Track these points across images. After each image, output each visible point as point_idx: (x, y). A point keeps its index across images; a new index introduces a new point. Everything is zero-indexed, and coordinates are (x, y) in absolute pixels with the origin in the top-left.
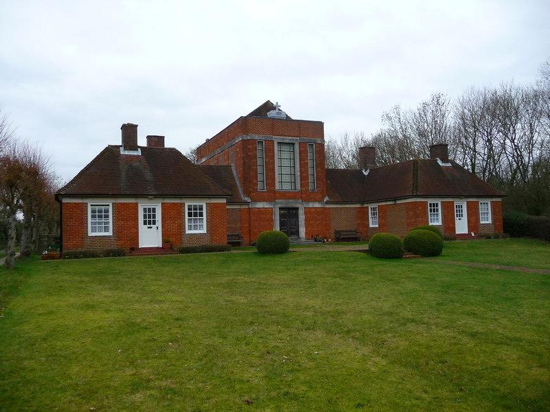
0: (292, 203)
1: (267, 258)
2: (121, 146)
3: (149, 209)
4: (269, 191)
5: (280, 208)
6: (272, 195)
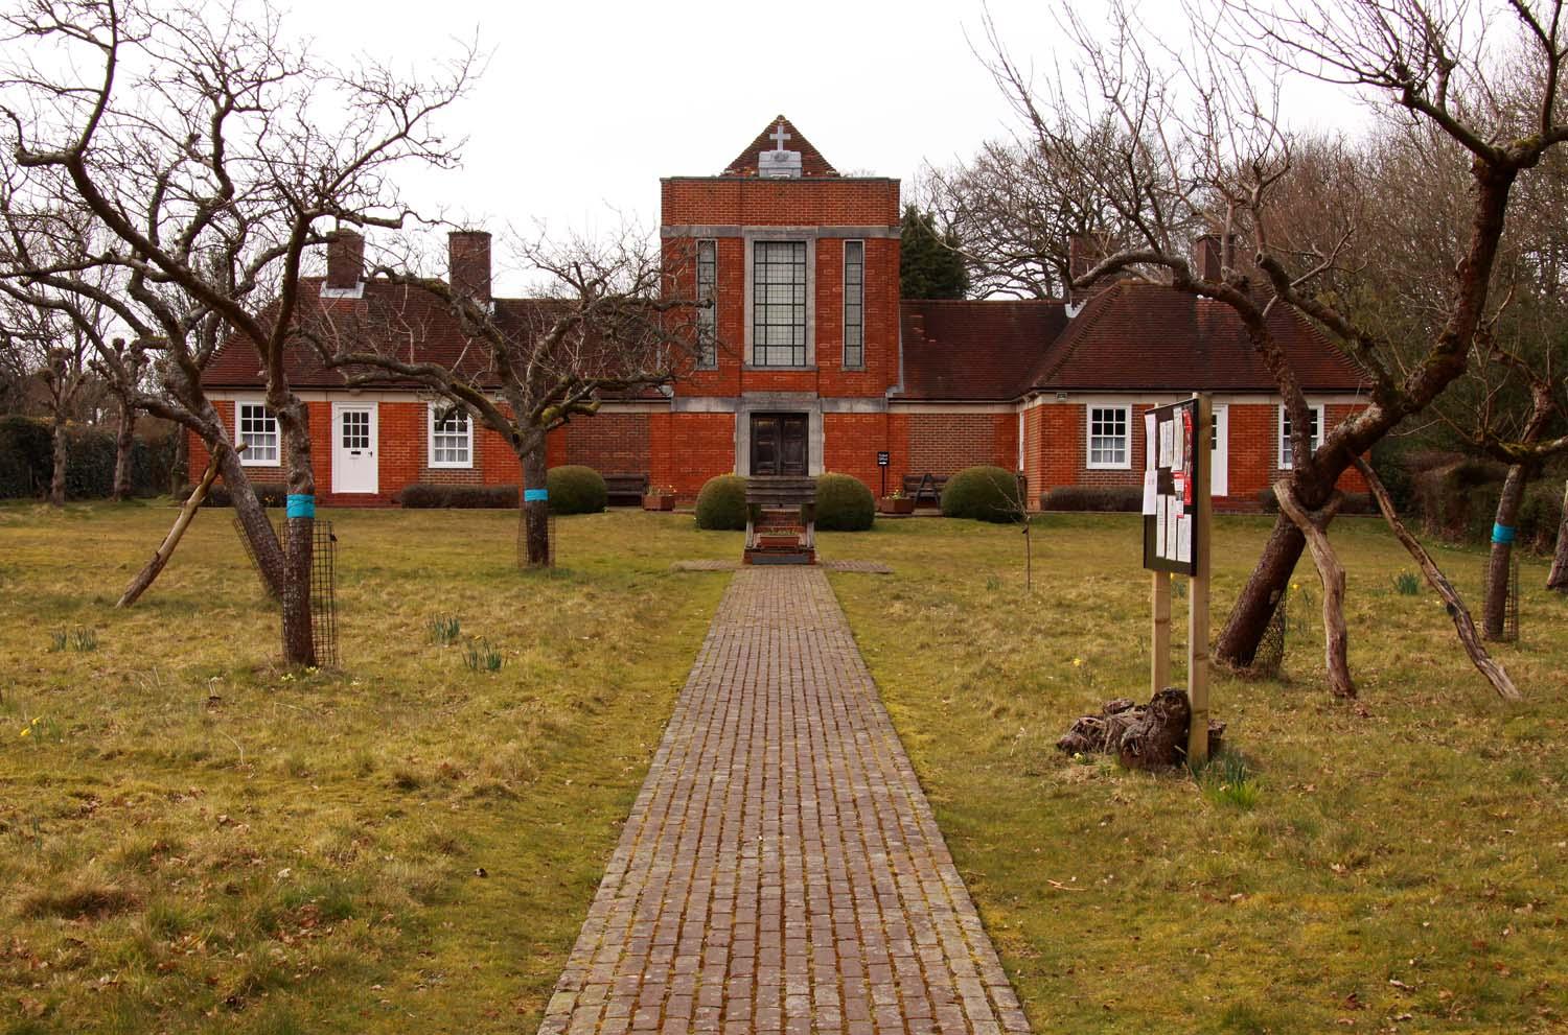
0: (788, 402)
1: (711, 533)
2: (323, 279)
3: (356, 415)
4: (724, 370)
5: (754, 415)
6: (733, 380)
